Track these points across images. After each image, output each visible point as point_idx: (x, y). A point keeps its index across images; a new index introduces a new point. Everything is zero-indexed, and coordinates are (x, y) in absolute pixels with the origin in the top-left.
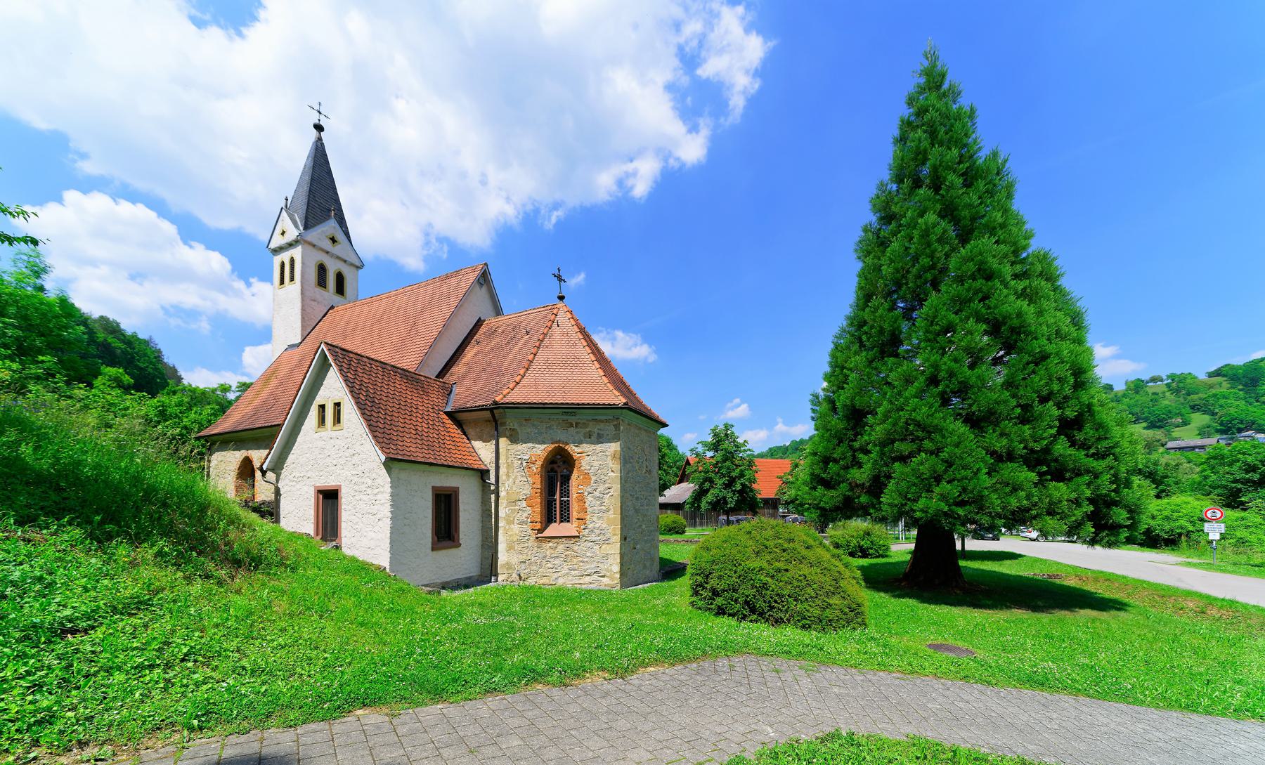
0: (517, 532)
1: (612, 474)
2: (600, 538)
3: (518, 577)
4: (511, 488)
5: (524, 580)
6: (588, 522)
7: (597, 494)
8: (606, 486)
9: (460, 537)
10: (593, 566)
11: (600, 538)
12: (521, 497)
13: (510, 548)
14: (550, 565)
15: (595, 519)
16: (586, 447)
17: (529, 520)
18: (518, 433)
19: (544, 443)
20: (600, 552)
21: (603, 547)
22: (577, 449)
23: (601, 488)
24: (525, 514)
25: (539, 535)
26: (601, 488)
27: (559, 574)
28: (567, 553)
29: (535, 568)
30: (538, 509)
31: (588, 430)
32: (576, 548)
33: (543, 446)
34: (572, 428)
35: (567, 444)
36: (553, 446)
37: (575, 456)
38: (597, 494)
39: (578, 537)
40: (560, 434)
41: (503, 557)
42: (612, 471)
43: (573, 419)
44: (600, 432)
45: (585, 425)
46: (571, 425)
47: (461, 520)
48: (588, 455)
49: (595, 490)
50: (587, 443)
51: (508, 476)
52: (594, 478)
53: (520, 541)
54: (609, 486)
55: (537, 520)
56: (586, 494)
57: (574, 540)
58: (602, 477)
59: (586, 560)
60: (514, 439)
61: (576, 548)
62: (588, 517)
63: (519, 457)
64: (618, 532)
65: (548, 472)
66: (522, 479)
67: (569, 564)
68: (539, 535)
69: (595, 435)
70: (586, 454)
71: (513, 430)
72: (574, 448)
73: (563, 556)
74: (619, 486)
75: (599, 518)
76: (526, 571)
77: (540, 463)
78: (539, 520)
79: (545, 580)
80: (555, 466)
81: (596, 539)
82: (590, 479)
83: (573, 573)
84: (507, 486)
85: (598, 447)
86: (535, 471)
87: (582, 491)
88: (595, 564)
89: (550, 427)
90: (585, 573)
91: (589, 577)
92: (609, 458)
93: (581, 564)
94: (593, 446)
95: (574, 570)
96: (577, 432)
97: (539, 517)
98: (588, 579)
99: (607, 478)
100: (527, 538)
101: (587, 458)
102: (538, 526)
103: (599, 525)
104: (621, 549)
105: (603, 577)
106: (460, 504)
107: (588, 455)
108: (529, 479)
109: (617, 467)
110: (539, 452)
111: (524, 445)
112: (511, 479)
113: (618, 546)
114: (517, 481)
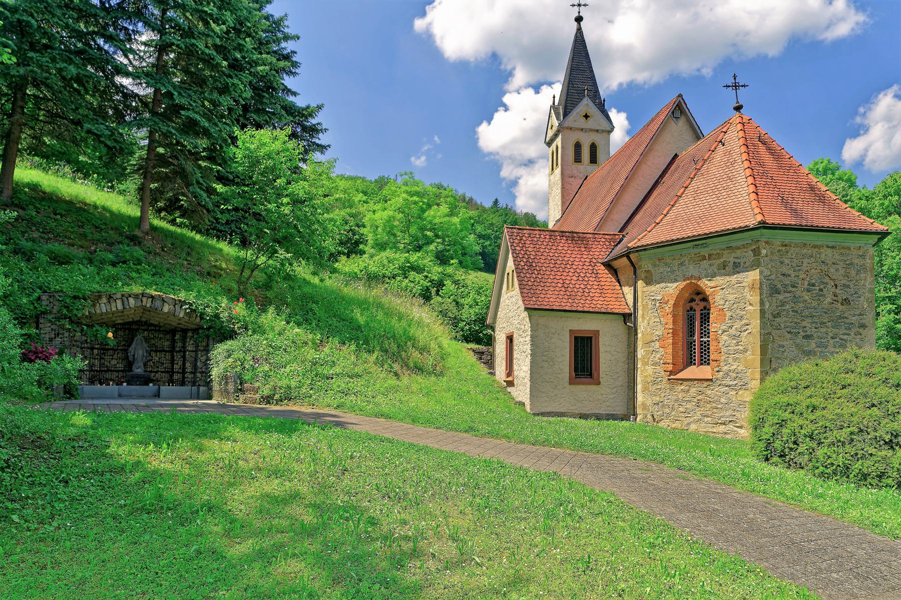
1: (750, 308)
3: (652, 419)
5: (657, 422)
7: (732, 331)
8: (744, 322)
10: (727, 414)
13: (645, 389)
14: (681, 409)
15: (730, 360)
16: (719, 280)
17: (662, 361)
18: (652, 275)
19: (676, 281)
22: (710, 284)
23: (737, 325)
24: (658, 356)
25: (672, 377)
26: (737, 325)
27: (691, 419)
29: (667, 411)
31: (722, 260)
32: (709, 392)
33: (675, 285)
34: (705, 261)
35: (700, 279)
36: (685, 283)
37: (708, 291)
38: (732, 331)
39: (711, 380)
40: (692, 270)
41: (640, 398)
42: (751, 304)
43: (705, 252)
44: (736, 260)
45: (719, 256)
46: (704, 258)
48: (723, 289)
50: (721, 275)
52: (728, 314)
53: (654, 383)
55: (669, 361)
56: (720, 332)
57: (706, 384)
59: (720, 406)
60: (649, 282)
63: (653, 298)
66: (655, 320)
67: (702, 409)
68: (672, 377)
69: (731, 264)
70: (719, 288)
71: (648, 271)
72: (707, 282)
73: (695, 400)
74: (759, 321)
76: (660, 413)
77: (672, 302)
78: (671, 361)
79: (677, 425)
81: (731, 383)
82: (725, 315)
83: (706, 419)
84: (642, 328)
85: (734, 278)
87: (715, 330)
88: (729, 413)
89: (682, 264)
90: (720, 421)
91: (724, 426)
92: (747, 289)
93: (715, 410)
94: (728, 278)
95: (707, 416)
96: (711, 265)
98: (722, 428)
99: (744, 313)
100: (660, 379)
101: (721, 292)
102: (670, 367)
103: (735, 367)
105: (741, 427)
107: (723, 289)
108: (662, 319)
110: (671, 291)
111: (658, 286)
114: (651, 322)
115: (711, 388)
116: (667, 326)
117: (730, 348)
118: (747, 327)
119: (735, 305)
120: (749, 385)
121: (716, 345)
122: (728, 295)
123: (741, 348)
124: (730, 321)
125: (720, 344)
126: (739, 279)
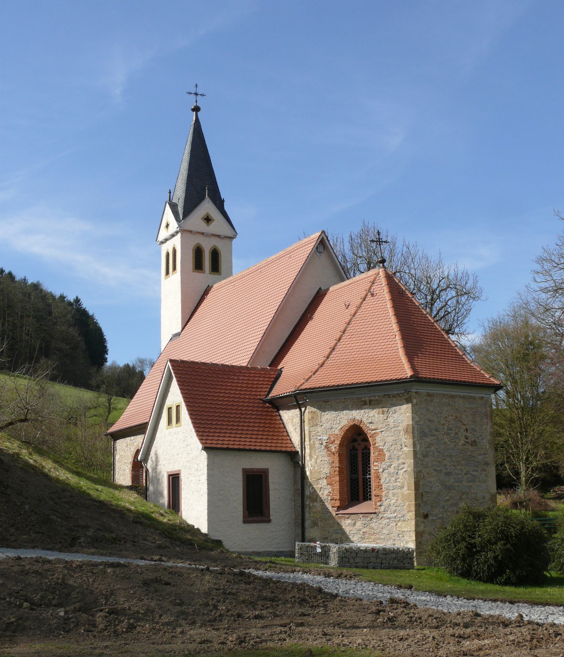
0: (320, 509)
1: (405, 449)
2: (395, 514)
4: (314, 468)
6: (384, 499)
9: (271, 514)
11: (395, 514)
12: (322, 476)
17: (329, 498)
20: (396, 529)
21: (399, 524)
26: (395, 464)
28: (364, 530)
30: (337, 486)
38: (392, 470)
42: (406, 446)
47: (272, 498)
49: (390, 466)
51: (311, 456)
52: (387, 454)
54: (403, 461)
56: (381, 470)
58: (395, 452)
59: (382, 537)
61: (373, 525)
62: (384, 493)
63: (320, 438)
64: (413, 508)
65: (351, 450)
66: (323, 459)
74: (412, 461)
75: (394, 495)
77: (338, 442)
78: (338, 497)
80: (355, 444)
82: (385, 455)
84: (310, 466)
86: (334, 450)
87: (377, 468)
92: (402, 433)
97: (338, 494)
99: (401, 453)
104: (417, 525)
106: (270, 484)
109: (410, 441)
110: (337, 432)
112: (313, 460)
113: (413, 523)
114: (318, 461)
115: (375, 521)
116: (333, 465)
117: (389, 484)
118: (403, 466)
119: (393, 447)
120: (406, 517)
121: (377, 481)
122: (387, 437)
123: (399, 484)
124: (389, 460)
125: (382, 481)
126: (395, 424)
